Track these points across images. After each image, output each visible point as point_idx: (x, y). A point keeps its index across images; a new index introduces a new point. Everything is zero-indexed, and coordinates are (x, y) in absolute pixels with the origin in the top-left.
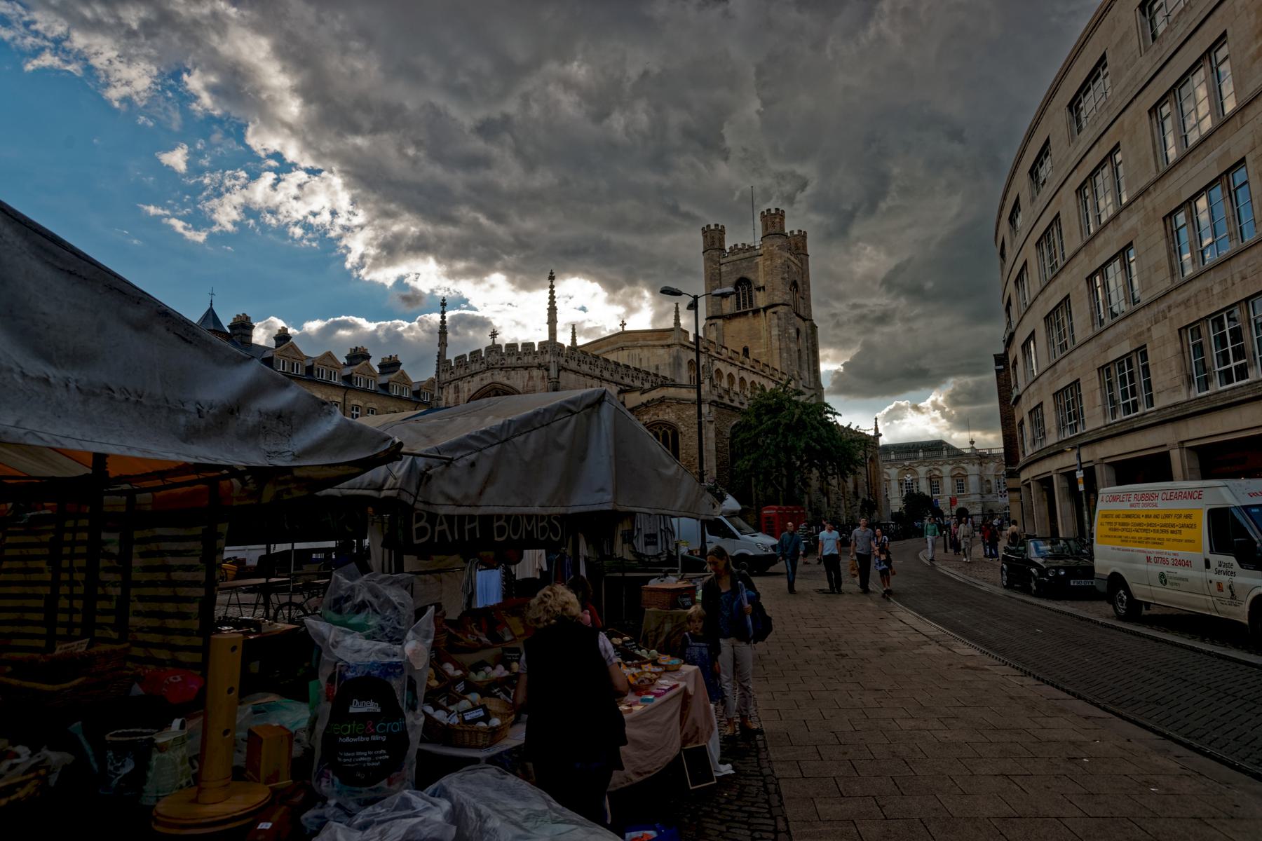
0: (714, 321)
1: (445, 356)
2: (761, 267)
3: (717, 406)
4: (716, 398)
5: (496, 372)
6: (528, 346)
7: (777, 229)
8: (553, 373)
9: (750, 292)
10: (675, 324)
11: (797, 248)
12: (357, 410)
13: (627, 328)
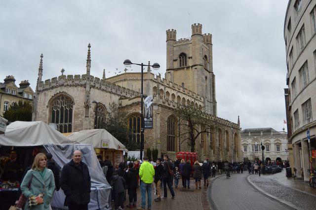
0: (170, 71)
1: (41, 79)
3: (162, 107)
4: (162, 103)
5: (63, 87)
6: (77, 77)
11: (207, 41)
12: (7, 104)
13: (127, 72)
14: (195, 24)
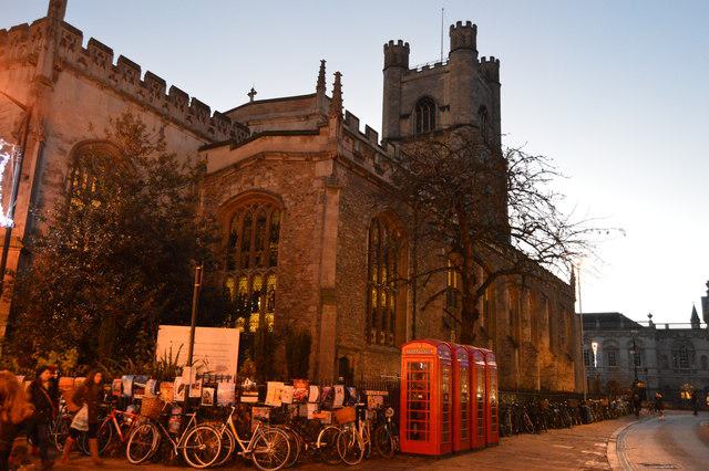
2: (446, 85)
3: (350, 169)
7: (467, 43)
8: (44, 68)
9: (433, 112)
10: (318, 88)
13: (256, 98)
14: (459, 23)
